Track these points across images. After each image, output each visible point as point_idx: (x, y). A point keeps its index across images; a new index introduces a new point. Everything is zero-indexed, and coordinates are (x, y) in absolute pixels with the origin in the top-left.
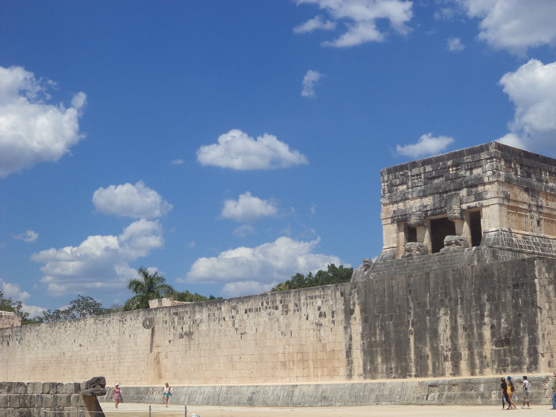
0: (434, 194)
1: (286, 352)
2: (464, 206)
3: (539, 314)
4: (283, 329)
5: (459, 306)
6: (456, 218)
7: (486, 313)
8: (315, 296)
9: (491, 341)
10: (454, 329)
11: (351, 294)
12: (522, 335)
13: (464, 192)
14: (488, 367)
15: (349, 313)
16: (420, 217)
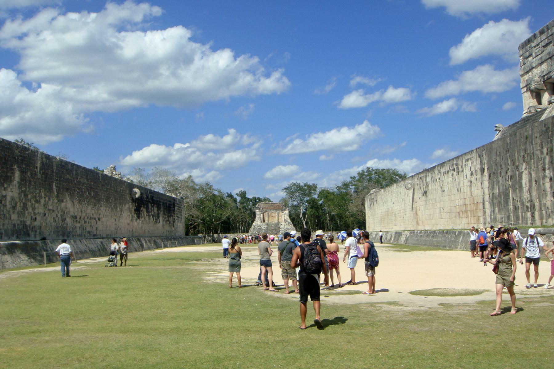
10: (530, 181)
15: (482, 170)
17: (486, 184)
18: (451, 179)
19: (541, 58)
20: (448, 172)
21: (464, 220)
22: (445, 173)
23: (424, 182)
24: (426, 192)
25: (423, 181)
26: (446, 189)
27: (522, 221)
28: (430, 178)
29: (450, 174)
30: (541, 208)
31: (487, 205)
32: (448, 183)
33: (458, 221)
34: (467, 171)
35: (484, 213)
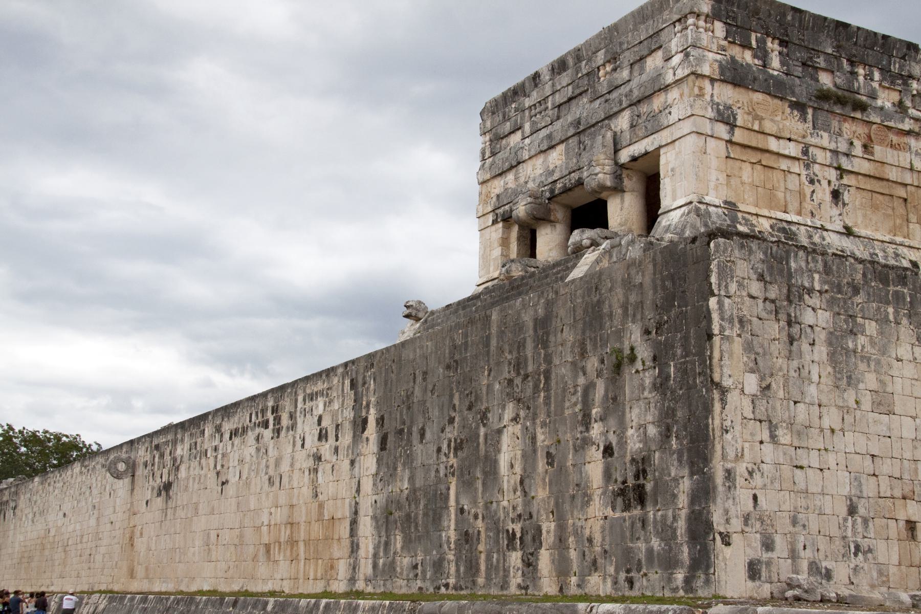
0: (567, 139)
1: (273, 523)
2: (624, 156)
3: (717, 406)
4: (271, 472)
5: (542, 394)
6: (603, 188)
7: (594, 411)
8: (317, 393)
9: (604, 493)
10: (529, 456)
11: (364, 383)
12: (673, 474)
13: (623, 122)
14: (596, 570)
15: (360, 424)
16: (536, 198)
17: (369, 463)
18: (253, 450)
19: (549, 137)
20: (245, 430)
21: (284, 568)
22: (234, 433)
23: (167, 458)
24: (168, 487)
25: (162, 456)
26: (233, 479)
27: (488, 578)
28: (187, 446)
29: (251, 436)
30: (561, 541)
31: (366, 527)
32: (241, 461)
33: (263, 570)
34: (307, 428)
35: (354, 548)
